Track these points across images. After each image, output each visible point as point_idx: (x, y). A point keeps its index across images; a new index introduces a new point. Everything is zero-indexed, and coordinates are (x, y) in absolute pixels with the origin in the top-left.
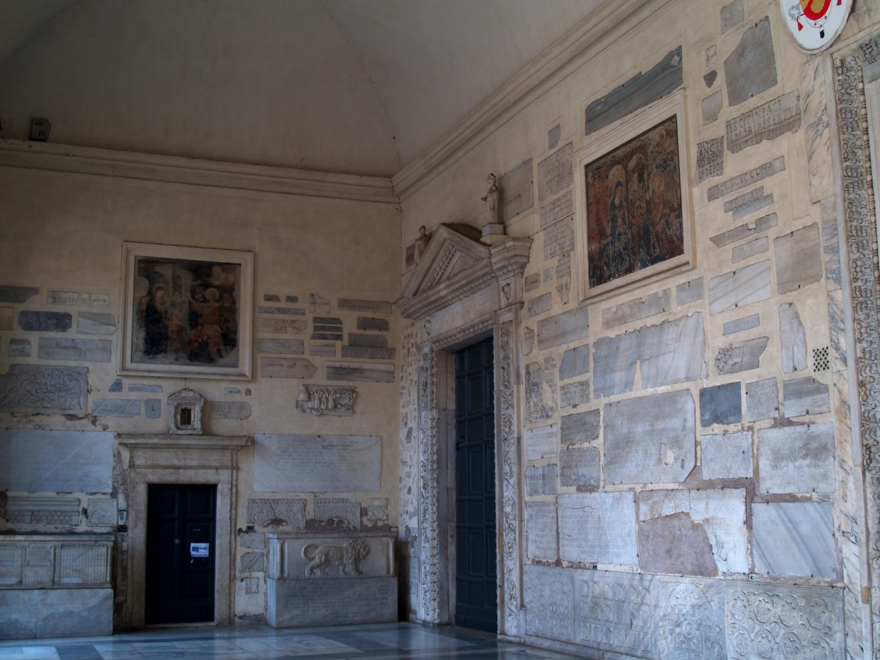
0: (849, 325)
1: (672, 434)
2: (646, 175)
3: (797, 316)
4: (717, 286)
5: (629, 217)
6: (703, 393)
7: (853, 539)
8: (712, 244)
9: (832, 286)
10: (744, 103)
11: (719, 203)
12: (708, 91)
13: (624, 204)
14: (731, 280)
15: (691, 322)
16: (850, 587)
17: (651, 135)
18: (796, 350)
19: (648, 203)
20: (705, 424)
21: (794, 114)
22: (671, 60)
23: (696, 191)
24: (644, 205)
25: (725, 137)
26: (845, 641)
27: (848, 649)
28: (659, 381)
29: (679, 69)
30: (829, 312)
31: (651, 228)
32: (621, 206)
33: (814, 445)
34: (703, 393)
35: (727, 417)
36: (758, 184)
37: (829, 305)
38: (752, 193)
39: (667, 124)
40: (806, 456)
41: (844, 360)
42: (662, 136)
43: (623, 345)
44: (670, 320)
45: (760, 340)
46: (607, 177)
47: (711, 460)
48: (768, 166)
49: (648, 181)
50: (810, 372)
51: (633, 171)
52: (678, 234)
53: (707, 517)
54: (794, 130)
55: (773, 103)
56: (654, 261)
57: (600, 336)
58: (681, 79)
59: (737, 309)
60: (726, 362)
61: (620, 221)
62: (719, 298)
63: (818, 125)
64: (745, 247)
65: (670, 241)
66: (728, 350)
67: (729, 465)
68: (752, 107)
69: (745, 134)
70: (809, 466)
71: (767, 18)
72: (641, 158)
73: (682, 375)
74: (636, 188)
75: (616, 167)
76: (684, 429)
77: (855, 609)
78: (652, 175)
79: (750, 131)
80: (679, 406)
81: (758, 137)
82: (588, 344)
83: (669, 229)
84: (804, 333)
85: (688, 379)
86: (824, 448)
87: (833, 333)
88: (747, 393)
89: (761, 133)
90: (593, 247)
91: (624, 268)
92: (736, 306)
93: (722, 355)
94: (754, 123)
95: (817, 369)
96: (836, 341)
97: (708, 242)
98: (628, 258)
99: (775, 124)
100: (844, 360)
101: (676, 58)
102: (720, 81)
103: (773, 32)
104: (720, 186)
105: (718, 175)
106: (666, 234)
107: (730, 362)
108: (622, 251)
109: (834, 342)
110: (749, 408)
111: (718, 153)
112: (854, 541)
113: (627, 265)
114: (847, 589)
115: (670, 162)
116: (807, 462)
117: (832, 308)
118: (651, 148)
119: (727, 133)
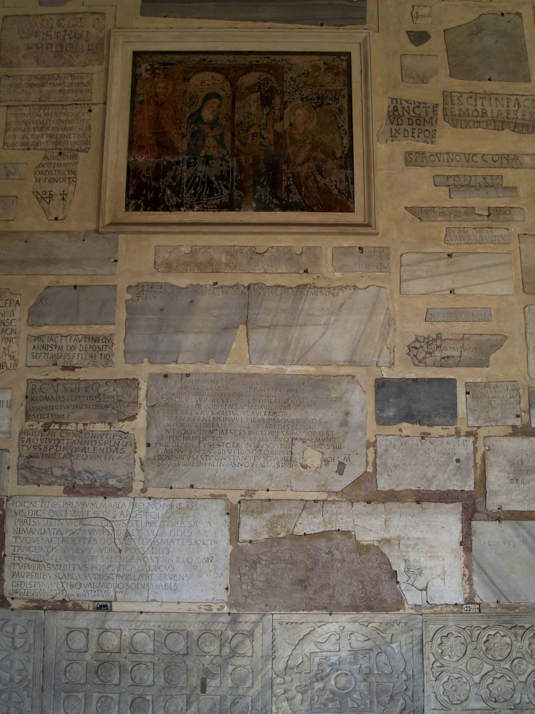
1: (319, 429)
4: (418, 263)
5: (233, 141)
10: (476, 82)
13: (223, 122)
14: (443, 262)
15: (363, 296)
17: (295, 59)
19: (279, 136)
24: (269, 136)
25: (441, 107)
28: (289, 358)
31: (284, 167)
32: (215, 123)
35: (430, 417)
38: (484, 177)
43: (204, 300)
45: (494, 338)
46: (186, 80)
47: (396, 467)
48: (512, 157)
51: (251, 89)
52: (342, 187)
53: (387, 536)
55: (524, 98)
56: (284, 208)
57: (147, 279)
61: (210, 141)
62: (419, 277)
64: (471, 231)
67: (430, 474)
68: (488, 91)
73: (341, 356)
74: (253, 110)
75: (208, 75)
76: (344, 423)
79: (486, 113)
80: (334, 395)
82: (116, 286)
85: (351, 363)
88: (468, 393)
90: (141, 159)
91: (218, 201)
93: (422, 344)
97: (402, 210)
98: (226, 192)
106: (317, 182)
108: (213, 179)
111: (427, 119)
113: (225, 199)
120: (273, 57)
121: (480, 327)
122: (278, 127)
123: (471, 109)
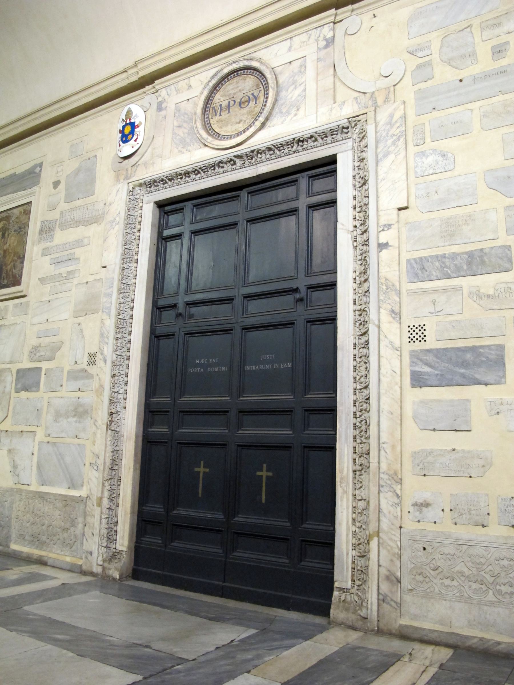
0: (111, 340)
2: (6, 235)
3: (82, 331)
6: (19, 371)
7: (95, 468)
8: (39, 282)
9: (105, 316)
11: (47, 258)
12: (54, 191)
16: (91, 497)
17: (15, 211)
18: (78, 352)
19: (5, 251)
20: (17, 391)
21: (100, 213)
22: (35, 169)
23: (35, 249)
26: (84, 529)
27: (85, 534)
29: (39, 175)
30: (101, 331)
31: (4, 267)
33: (81, 409)
34: (19, 371)
36: (72, 251)
37: (101, 327)
39: (25, 206)
40: (75, 415)
41: (105, 361)
42: (21, 213)
44: (6, 324)
45: (58, 343)
48: (80, 241)
49: (7, 238)
50: (84, 366)
52: (20, 273)
53: (10, 448)
54: (99, 223)
55: (90, 205)
58: (39, 181)
59: (47, 323)
60: (35, 354)
63: (113, 222)
65: (14, 276)
66: (38, 347)
69: (70, 220)
70: (76, 422)
71: (96, 156)
72: (5, 224)
77: (92, 510)
78: (10, 235)
80: (3, 378)
81: (77, 223)
83: (15, 269)
84: (84, 342)
85: (11, 362)
86: (86, 412)
87: (101, 344)
88: (45, 374)
89: (80, 221)
92: (47, 321)
94: (77, 215)
95: (89, 364)
96: (102, 349)
97: (37, 280)
99: (88, 217)
100: (105, 361)
101: (38, 169)
102: (62, 187)
103: (98, 165)
104: (50, 248)
105: (50, 242)
106: (12, 272)
107: (38, 355)
109: (101, 350)
110: (45, 384)
111: (52, 229)
112: (96, 469)
114: (88, 498)
115: (22, 229)
116: (75, 419)
117: (103, 329)
118: (13, 219)
119: (60, 218)
120: (8, 212)
121: (54, 339)
122: (5, 248)
123: (69, 217)
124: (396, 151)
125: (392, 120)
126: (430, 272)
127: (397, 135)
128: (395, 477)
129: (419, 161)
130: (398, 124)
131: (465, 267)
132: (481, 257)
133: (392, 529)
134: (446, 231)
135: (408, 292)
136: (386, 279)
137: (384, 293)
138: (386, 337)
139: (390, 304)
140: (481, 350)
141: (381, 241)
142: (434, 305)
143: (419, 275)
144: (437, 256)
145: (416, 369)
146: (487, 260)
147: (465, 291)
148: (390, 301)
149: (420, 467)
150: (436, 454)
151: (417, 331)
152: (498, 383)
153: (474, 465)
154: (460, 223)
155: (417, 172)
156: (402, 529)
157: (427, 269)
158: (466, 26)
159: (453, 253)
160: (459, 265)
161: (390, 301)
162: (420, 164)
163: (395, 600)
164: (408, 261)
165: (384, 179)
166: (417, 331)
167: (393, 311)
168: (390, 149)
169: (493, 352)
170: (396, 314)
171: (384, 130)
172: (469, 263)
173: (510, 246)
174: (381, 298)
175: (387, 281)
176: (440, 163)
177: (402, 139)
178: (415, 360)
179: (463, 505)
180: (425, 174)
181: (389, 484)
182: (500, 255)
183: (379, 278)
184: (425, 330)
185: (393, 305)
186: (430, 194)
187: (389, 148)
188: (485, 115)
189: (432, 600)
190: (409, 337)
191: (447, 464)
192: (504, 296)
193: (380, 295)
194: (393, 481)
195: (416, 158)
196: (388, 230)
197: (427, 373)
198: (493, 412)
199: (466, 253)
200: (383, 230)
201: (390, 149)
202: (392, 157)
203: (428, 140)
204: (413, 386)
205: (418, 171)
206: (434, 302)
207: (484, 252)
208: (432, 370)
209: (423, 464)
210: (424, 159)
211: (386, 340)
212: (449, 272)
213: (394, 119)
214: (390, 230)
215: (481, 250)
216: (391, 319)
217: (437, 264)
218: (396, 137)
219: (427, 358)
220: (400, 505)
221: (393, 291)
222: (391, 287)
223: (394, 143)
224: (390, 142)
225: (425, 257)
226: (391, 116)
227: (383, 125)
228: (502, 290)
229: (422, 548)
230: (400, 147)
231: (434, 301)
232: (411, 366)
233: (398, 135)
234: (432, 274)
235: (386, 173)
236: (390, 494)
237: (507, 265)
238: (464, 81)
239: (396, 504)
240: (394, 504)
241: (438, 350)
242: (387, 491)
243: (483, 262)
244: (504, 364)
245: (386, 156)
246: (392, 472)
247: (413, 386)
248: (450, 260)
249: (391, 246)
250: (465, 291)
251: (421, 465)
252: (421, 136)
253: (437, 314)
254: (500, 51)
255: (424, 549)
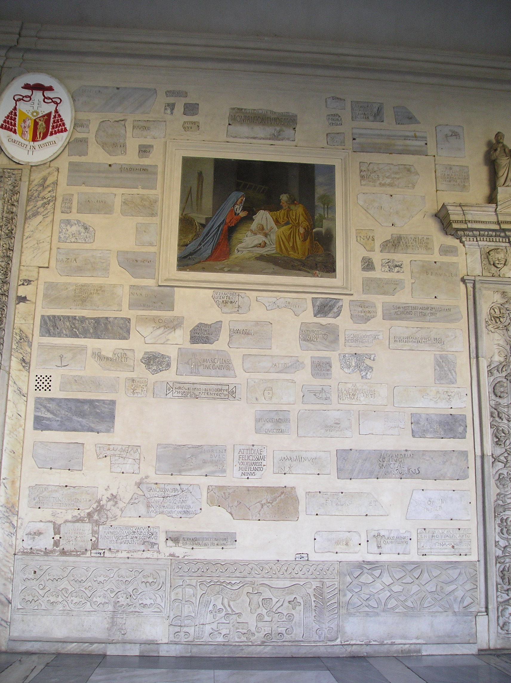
124: (44, 214)
125: (44, 183)
126: (61, 330)
127: (47, 199)
128: (13, 510)
129: (64, 227)
130: (50, 189)
131: (91, 331)
132: (106, 324)
133: (7, 557)
134: (79, 296)
135: (39, 344)
136: (20, 330)
137: (17, 343)
138: (15, 383)
139: (21, 353)
140: (97, 403)
141: (19, 295)
142: (61, 359)
143: (51, 331)
144: (68, 317)
145: (39, 414)
146: (110, 328)
147: (89, 352)
148: (21, 351)
149: (35, 501)
150: (50, 490)
151: (43, 380)
152: (108, 431)
153: (82, 500)
154: (92, 291)
155: (61, 238)
156: (16, 556)
157: (59, 327)
158: (122, 119)
159: (83, 317)
160: (86, 328)
161: (21, 351)
162: (64, 231)
163: (5, 619)
164: (43, 316)
165: (30, 237)
166: (43, 380)
167: (24, 360)
168: (39, 210)
169: (106, 406)
170: (26, 364)
171: (37, 190)
172: (95, 328)
173: (130, 319)
174: (14, 347)
175: (22, 332)
176: (82, 234)
177: (51, 204)
178: (40, 406)
179: (71, 533)
180: (67, 241)
181: (6, 516)
182: (121, 325)
183: (14, 328)
184: (50, 381)
185: (24, 355)
186: (69, 260)
187: (38, 209)
188: (125, 203)
189: (39, 616)
190: (36, 386)
191: (60, 498)
192: (120, 360)
193: (13, 344)
194: (10, 513)
195: (62, 225)
196: (28, 285)
197: (48, 419)
198: (101, 456)
199: (94, 319)
200: (23, 284)
201: (39, 210)
202: (40, 218)
203: (74, 210)
204: (35, 428)
205: (62, 237)
206: (61, 357)
207: (109, 320)
208: (54, 417)
209: (39, 498)
210: (68, 227)
211: (15, 385)
212: (77, 332)
213: (48, 183)
214: (29, 286)
215: (107, 318)
216: (21, 367)
217: (68, 324)
218: (46, 200)
219: (51, 405)
220: (15, 534)
221: (26, 342)
222: (24, 338)
223: (44, 205)
224: (40, 203)
225: (58, 316)
226: (45, 179)
227: (36, 186)
228: (119, 355)
229: (33, 572)
230: (48, 210)
231: (61, 356)
232: (35, 411)
233: (49, 199)
234: (63, 332)
235: (32, 231)
236: (7, 524)
237: (125, 334)
238: (113, 167)
239: (12, 533)
240: (10, 534)
241: (61, 400)
242: (4, 522)
243: (107, 329)
244: (114, 416)
245: (34, 216)
246: (10, 506)
247: (35, 428)
248: (80, 322)
249: (28, 300)
250: (89, 352)
251: (37, 499)
252: (69, 205)
253: (63, 368)
254: (145, 151)
255: (35, 572)
